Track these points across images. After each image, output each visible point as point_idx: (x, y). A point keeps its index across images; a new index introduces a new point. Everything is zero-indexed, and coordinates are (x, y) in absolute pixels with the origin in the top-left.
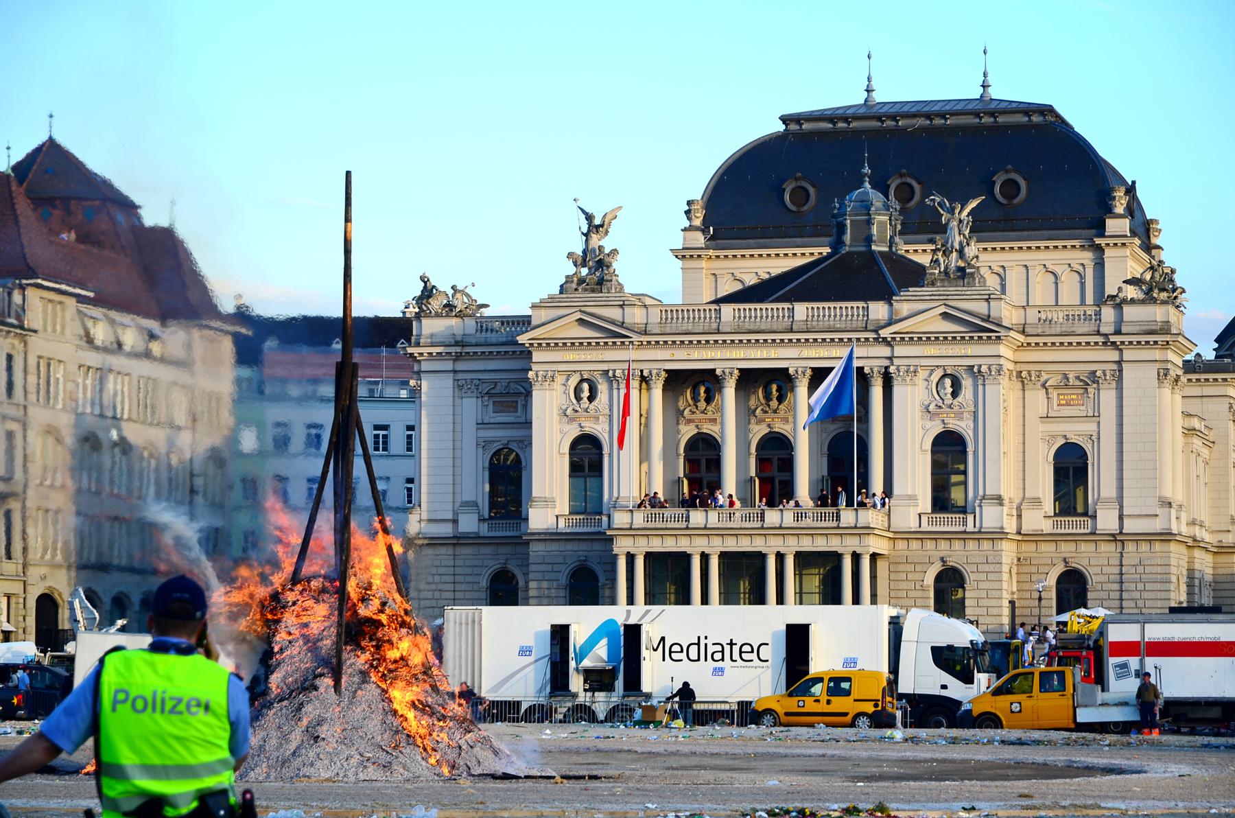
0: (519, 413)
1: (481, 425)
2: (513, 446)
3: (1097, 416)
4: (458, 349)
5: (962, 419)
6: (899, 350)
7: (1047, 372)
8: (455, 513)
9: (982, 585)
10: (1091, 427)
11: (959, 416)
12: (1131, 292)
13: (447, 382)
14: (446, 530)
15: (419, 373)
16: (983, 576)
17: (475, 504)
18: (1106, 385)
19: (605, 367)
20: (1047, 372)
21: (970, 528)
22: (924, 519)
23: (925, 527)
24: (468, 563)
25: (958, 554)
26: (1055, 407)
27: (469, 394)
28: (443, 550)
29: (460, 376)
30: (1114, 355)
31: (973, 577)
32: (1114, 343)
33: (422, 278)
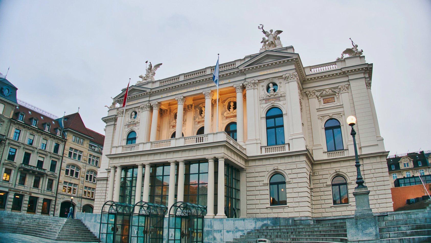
3: (341, 106)
5: (280, 101)
6: (248, 76)
7: (318, 91)
9: (295, 181)
10: (341, 110)
11: (278, 98)
12: (347, 56)
16: (295, 176)
18: (344, 91)
20: (318, 91)
21: (287, 151)
22: (263, 149)
23: (264, 153)
25: (282, 165)
26: (323, 104)
30: (346, 79)
31: (290, 176)
32: (344, 73)
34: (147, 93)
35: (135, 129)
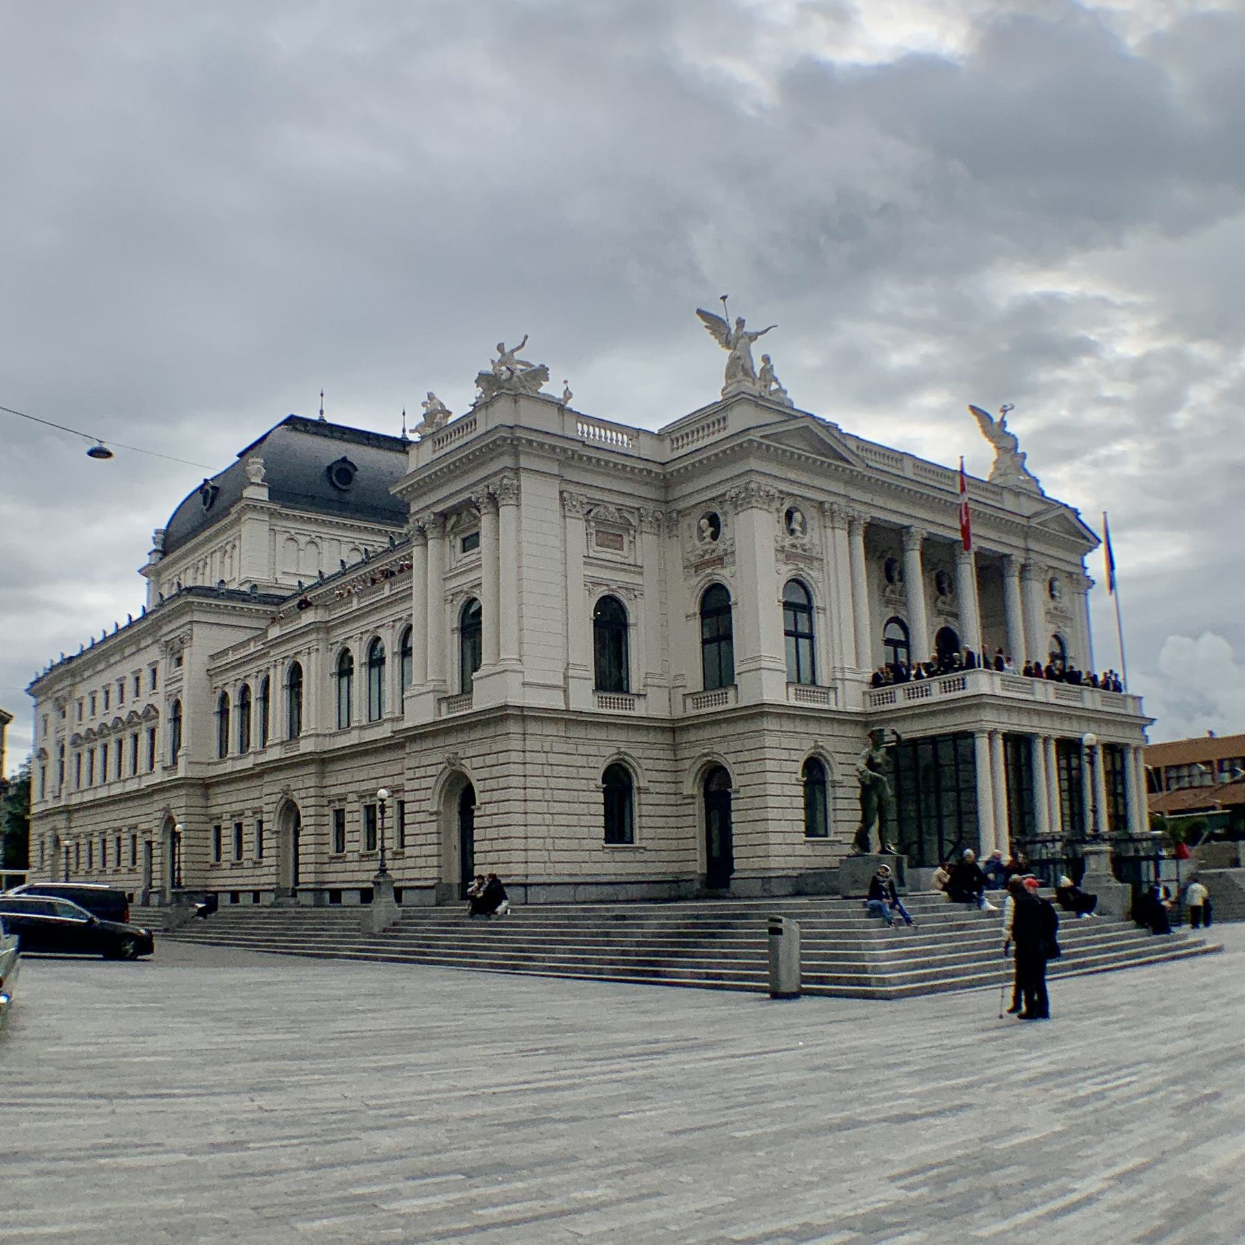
0: (625, 553)
1: (589, 561)
2: (622, 596)
4: (577, 447)
6: (1033, 545)
8: (566, 677)
13: (551, 490)
14: (554, 701)
15: (517, 471)
17: (582, 667)
19: (820, 497)
24: (582, 750)
27: (577, 515)
28: (550, 729)
29: (565, 486)
33: (500, 347)
34: (852, 471)
35: (812, 575)
